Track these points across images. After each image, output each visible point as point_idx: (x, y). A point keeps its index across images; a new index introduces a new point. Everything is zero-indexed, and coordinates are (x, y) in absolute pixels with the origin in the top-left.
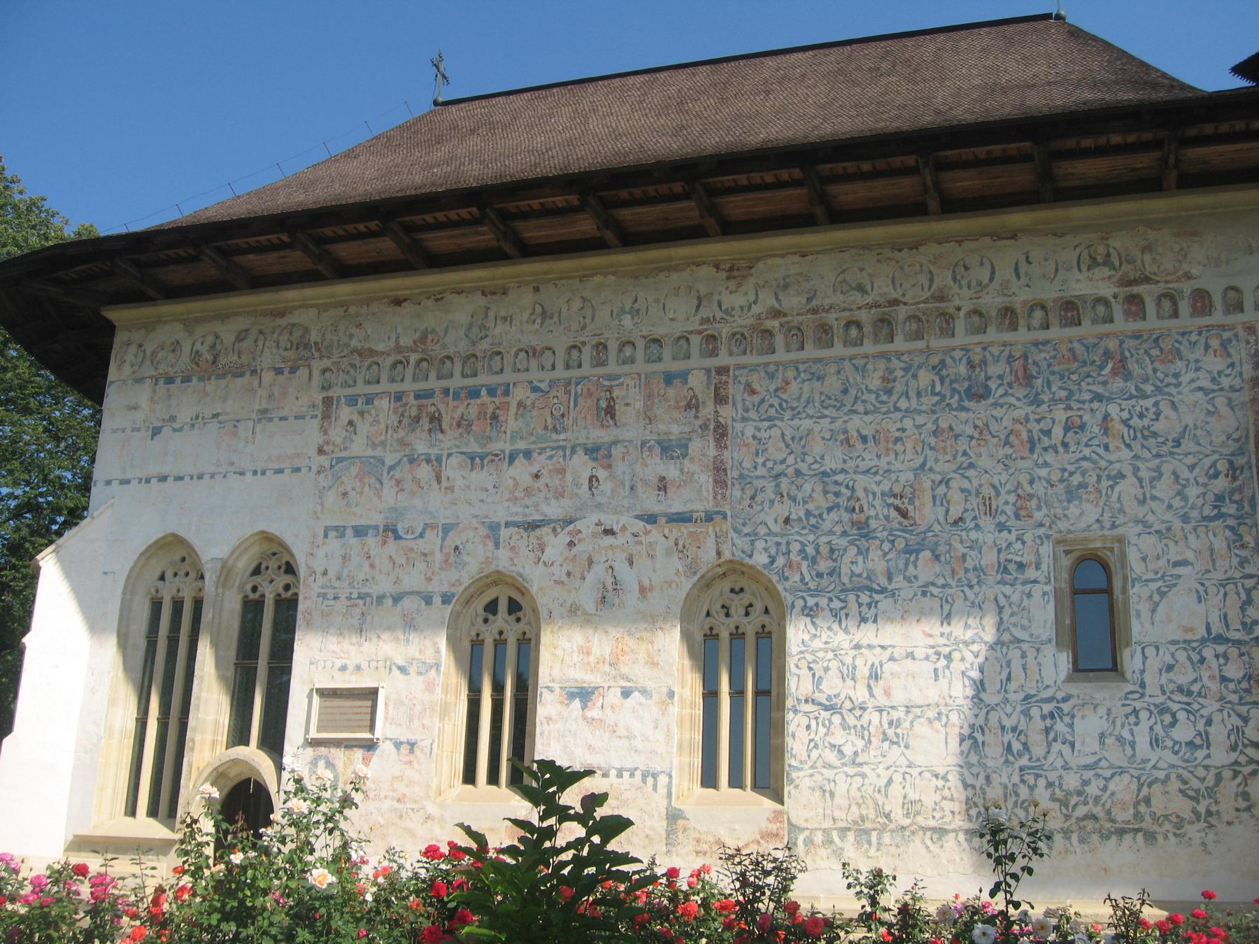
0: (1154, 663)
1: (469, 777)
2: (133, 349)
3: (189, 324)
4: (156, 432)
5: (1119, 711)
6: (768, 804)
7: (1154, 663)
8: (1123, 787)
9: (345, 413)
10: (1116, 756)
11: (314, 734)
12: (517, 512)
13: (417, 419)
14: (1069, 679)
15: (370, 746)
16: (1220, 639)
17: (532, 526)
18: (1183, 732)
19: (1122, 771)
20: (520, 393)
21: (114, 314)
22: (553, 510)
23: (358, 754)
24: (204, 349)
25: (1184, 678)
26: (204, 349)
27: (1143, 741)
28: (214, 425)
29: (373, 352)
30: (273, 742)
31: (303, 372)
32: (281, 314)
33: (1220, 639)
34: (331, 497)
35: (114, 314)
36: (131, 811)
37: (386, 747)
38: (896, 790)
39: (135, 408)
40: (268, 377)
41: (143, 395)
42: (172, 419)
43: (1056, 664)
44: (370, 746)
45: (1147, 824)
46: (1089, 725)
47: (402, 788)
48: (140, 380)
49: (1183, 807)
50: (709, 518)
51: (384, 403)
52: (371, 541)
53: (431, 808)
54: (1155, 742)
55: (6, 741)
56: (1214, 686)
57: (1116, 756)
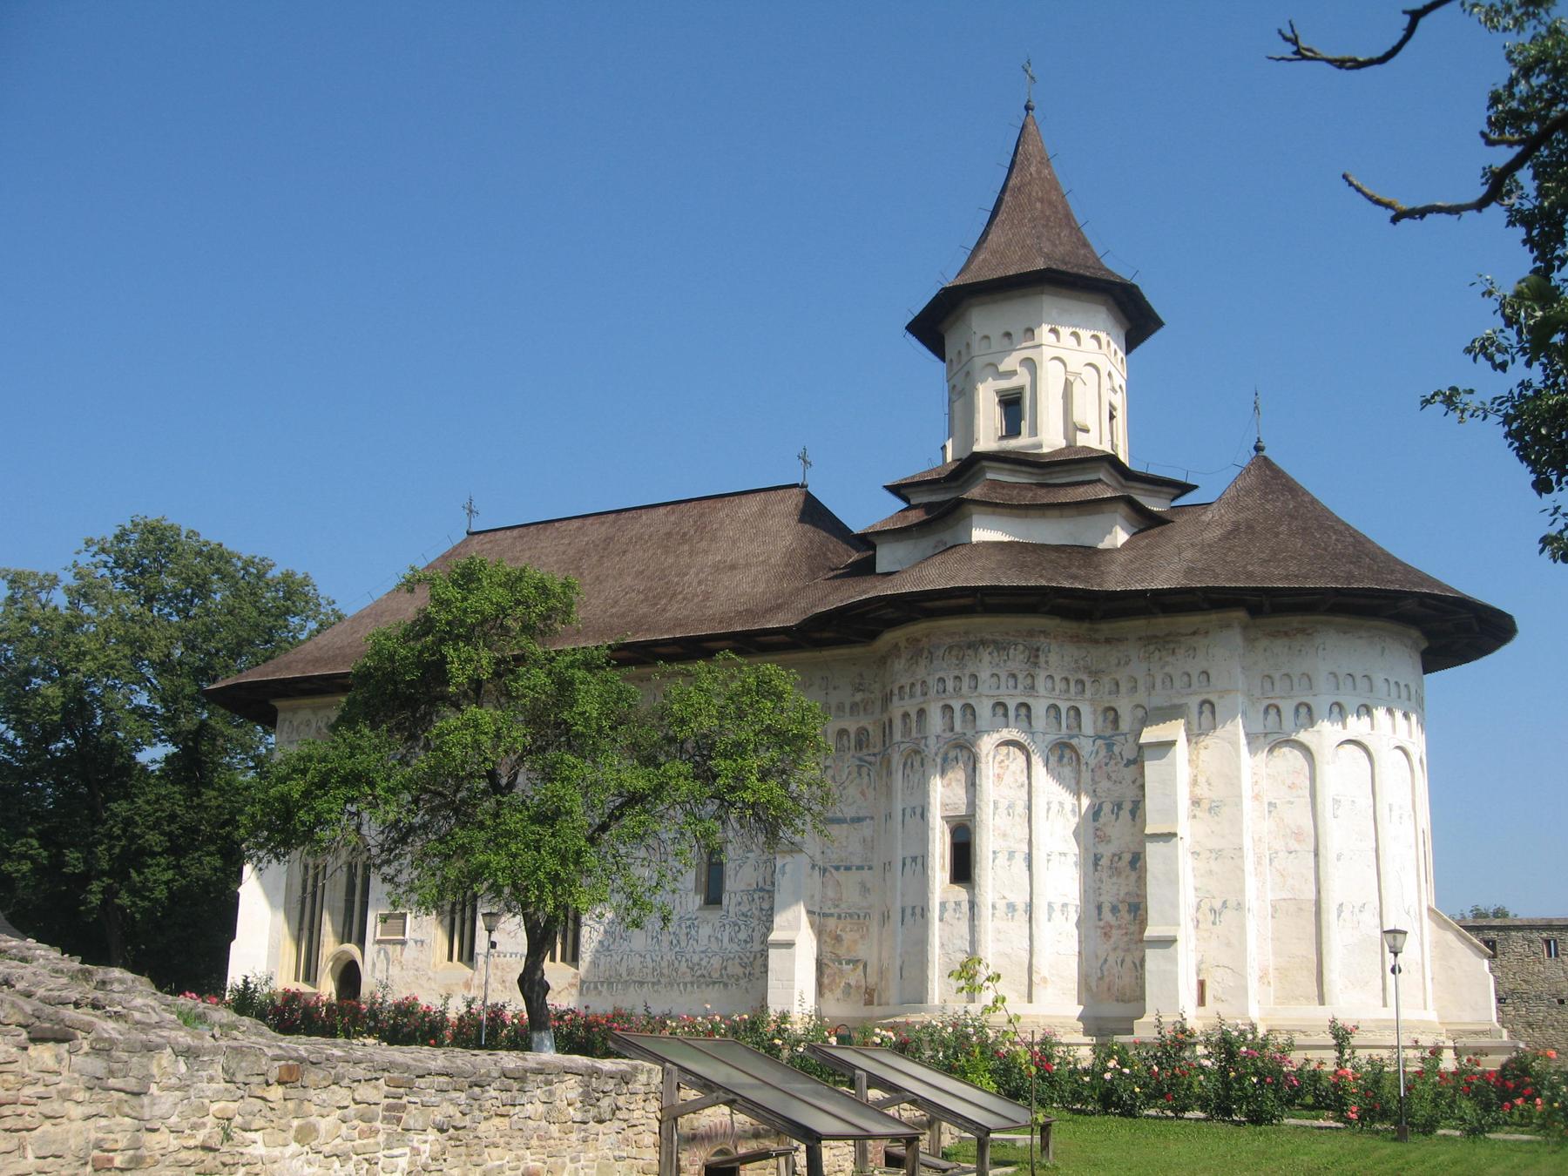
0: (734, 901)
1: (450, 958)
3: (315, 710)
5: (717, 924)
6: (573, 970)
7: (734, 901)
8: (716, 962)
10: (714, 946)
11: (378, 937)
14: (700, 909)
15: (403, 943)
16: (762, 890)
18: (743, 936)
19: (715, 954)
21: (278, 704)
23: (399, 947)
25: (744, 910)
27: (726, 940)
30: (361, 942)
33: (762, 890)
35: (278, 704)
36: (297, 979)
37: (411, 943)
38: (624, 964)
43: (699, 900)
44: (403, 943)
45: (725, 979)
46: (705, 931)
47: (418, 964)
49: (740, 971)
53: (431, 974)
54: (731, 940)
55: (233, 944)
56: (757, 913)
57: (714, 946)
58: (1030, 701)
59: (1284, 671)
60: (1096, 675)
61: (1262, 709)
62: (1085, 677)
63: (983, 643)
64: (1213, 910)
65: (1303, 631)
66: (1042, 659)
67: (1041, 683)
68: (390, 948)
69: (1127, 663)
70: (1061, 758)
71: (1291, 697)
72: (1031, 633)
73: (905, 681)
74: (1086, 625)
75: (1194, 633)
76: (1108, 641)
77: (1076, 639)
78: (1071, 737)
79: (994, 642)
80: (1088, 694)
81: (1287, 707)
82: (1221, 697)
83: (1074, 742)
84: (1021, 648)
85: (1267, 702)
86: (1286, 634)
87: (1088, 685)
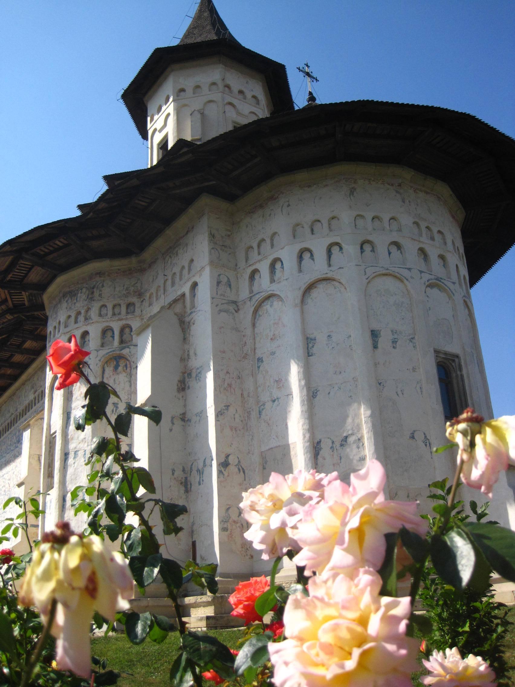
58: (89, 328)
59: (260, 238)
60: (140, 295)
61: (247, 276)
62: (134, 300)
63: (64, 296)
64: (198, 470)
65: (272, 198)
66: (96, 294)
67: (94, 313)
69: (157, 277)
70: (116, 368)
71: (266, 257)
72: (91, 277)
74: (134, 260)
75: (187, 233)
76: (150, 266)
77: (128, 273)
78: (124, 348)
79: (70, 292)
80: (138, 312)
81: (264, 267)
82: (200, 275)
83: (125, 352)
84: (84, 290)
85: (249, 270)
86: (261, 206)
87: (137, 305)
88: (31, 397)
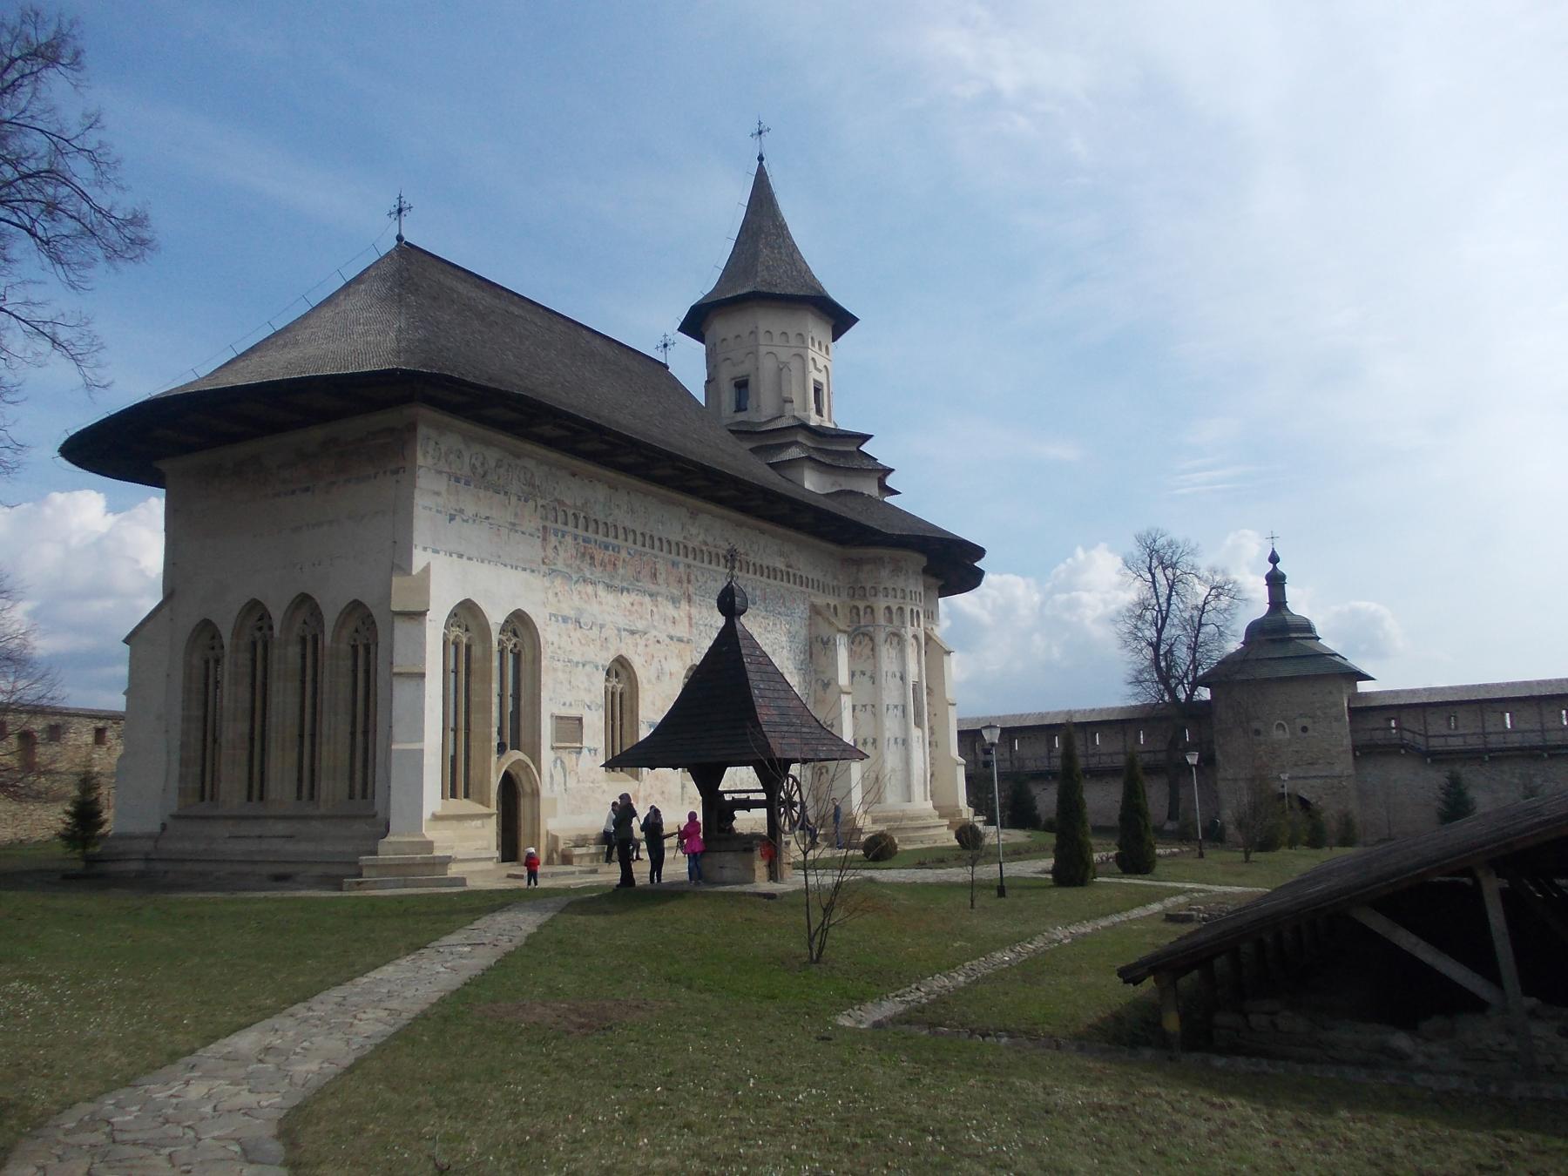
2: (432, 443)
4: (452, 518)
9: (553, 540)
12: (622, 622)
13: (583, 555)
17: (633, 633)
20: (624, 554)
22: (640, 625)
24: (478, 464)
26: (478, 464)
28: (486, 523)
29: (564, 504)
31: (531, 503)
32: (518, 457)
34: (550, 595)
37: (585, 751)
39: (438, 494)
40: (514, 499)
41: (441, 484)
42: (462, 511)
48: (440, 472)
50: (688, 642)
51: (569, 539)
52: (570, 626)
68: (564, 755)
73: (889, 585)
88: (780, 564)
